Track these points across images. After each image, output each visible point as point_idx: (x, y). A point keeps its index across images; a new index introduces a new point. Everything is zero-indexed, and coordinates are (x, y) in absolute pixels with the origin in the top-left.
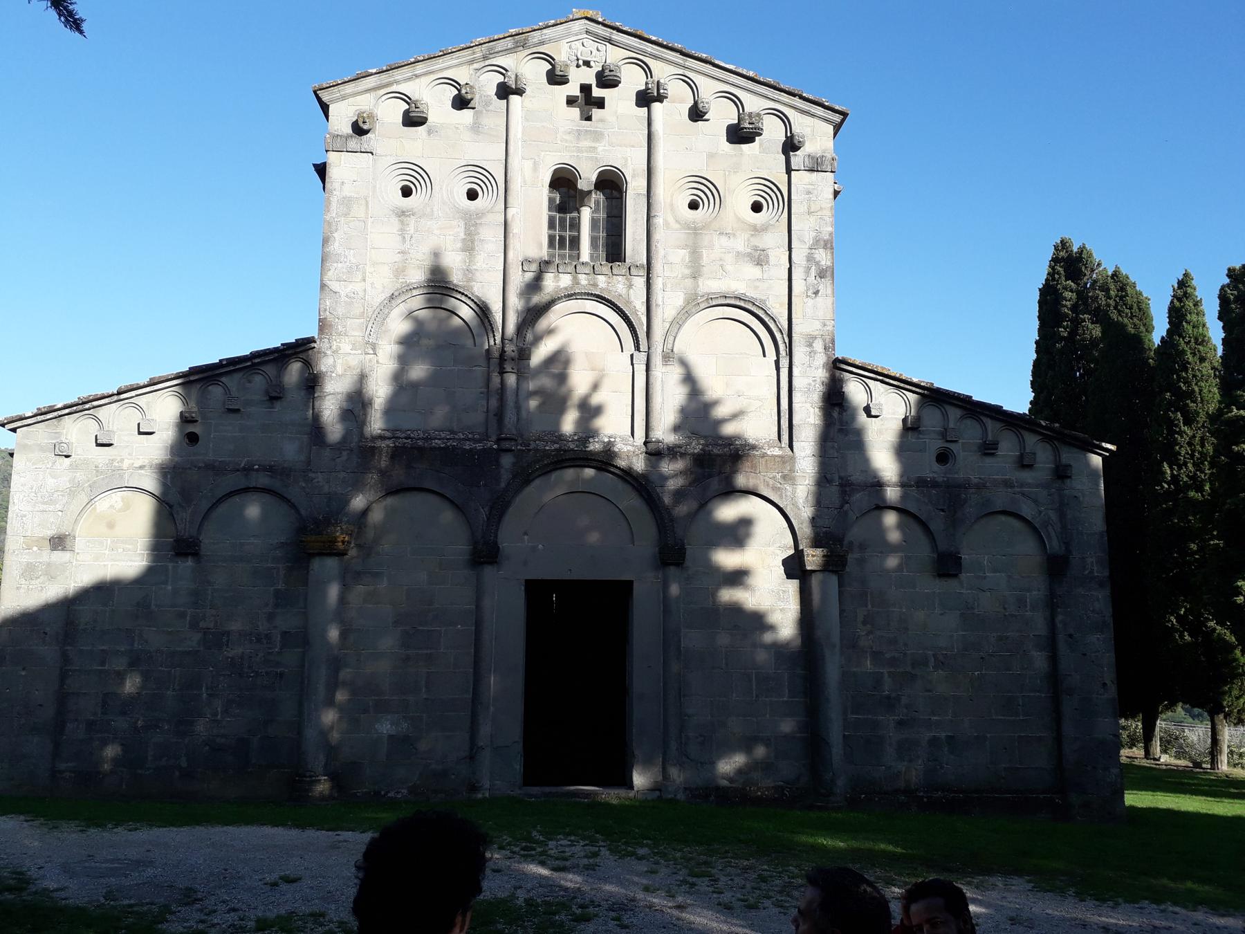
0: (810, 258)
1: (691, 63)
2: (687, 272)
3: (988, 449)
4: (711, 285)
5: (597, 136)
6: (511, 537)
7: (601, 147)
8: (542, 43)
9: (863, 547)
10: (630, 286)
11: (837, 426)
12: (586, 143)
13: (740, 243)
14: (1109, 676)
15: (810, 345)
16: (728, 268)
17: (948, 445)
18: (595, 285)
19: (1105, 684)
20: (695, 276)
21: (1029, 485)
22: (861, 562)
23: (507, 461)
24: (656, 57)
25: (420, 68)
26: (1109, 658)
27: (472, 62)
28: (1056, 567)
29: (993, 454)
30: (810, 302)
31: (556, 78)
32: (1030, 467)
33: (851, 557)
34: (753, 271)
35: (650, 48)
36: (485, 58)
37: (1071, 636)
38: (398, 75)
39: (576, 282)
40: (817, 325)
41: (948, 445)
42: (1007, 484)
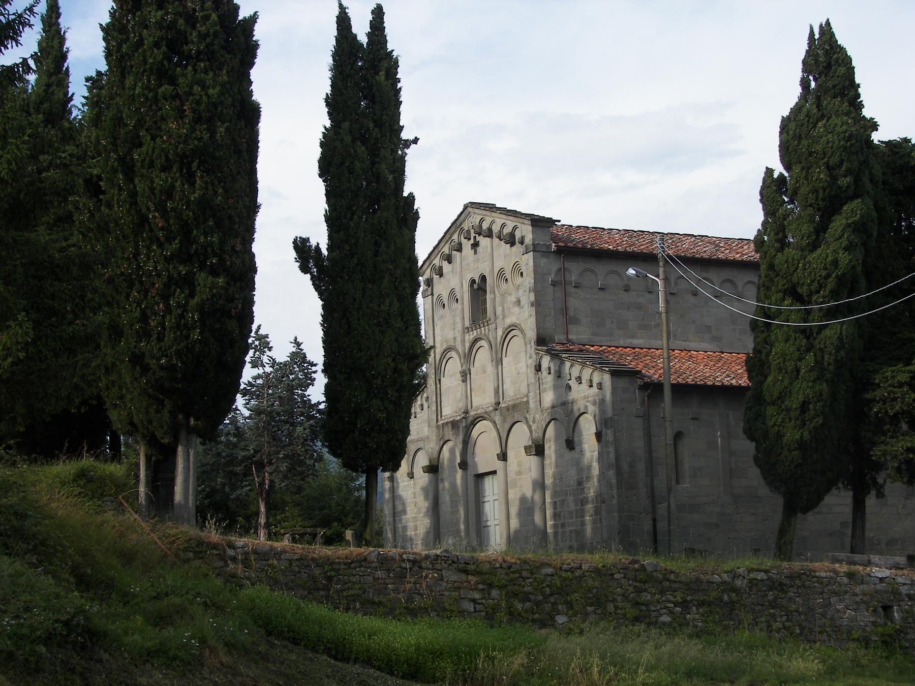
5: (478, 260)
8: (461, 224)
25: (436, 251)
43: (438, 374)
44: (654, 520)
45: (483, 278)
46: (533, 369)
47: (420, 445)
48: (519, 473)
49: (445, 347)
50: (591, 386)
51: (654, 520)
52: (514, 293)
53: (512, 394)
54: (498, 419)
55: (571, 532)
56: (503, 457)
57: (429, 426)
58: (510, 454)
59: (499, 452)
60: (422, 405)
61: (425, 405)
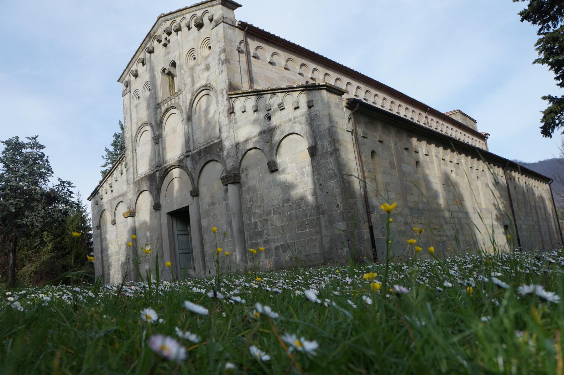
0: (220, 59)
1: (184, 12)
2: (191, 85)
3: (281, 107)
4: (198, 85)
5: (168, 53)
6: (163, 202)
7: (170, 56)
8: (154, 33)
9: (246, 169)
10: (179, 98)
11: (234, 121)
12: (167, 57)
13: (203, 66)
14: (339, 201)
15: (222, 93)
16: (201, 76)
17: (268, 112)
18: (172, 103)
19: (338, 205)
20: (193, 86)
21: (298, 117)
22: (247, 175)
23: (158, 174)
24: (177, 17)
25: (134, 60)
26: (337, 191)
27: (143, 50)
28: (313, 151)
29: (284, 108)
30: (220, 76)
31: (159, 41)
32: (297, 108)
33: (243, 176)
34: (206, 74)
35: (174, 15)
36: (145, 47)
37: (321, 185)
38: (130, 66)
39: (168, 104)
40: (224, 84)
41: (268, 112)
42: (290, 120)
43: (134, 145)
44: (371, 228)
45: (174, 64)
46: (226, 113)
47: (121, 199)
48: (213, 204)
49: (140, 124)
50: (296, 108)
51: (371, 228)
52: (204, 62)
53: (202, 141)
54: (189, 163)
55: (277, 248)
56: (195, 193)
57: (128, 184)
58: (203, 190)
59: (191, 189)
60: (122, 171)
61: (124, 171)
